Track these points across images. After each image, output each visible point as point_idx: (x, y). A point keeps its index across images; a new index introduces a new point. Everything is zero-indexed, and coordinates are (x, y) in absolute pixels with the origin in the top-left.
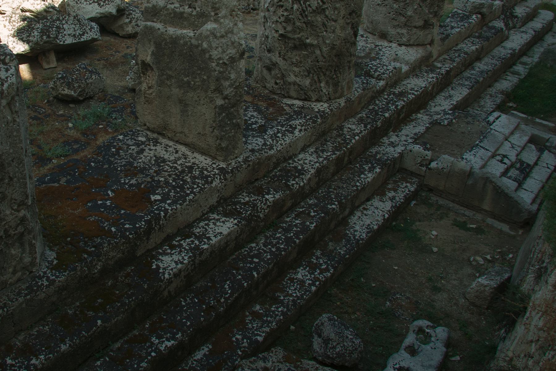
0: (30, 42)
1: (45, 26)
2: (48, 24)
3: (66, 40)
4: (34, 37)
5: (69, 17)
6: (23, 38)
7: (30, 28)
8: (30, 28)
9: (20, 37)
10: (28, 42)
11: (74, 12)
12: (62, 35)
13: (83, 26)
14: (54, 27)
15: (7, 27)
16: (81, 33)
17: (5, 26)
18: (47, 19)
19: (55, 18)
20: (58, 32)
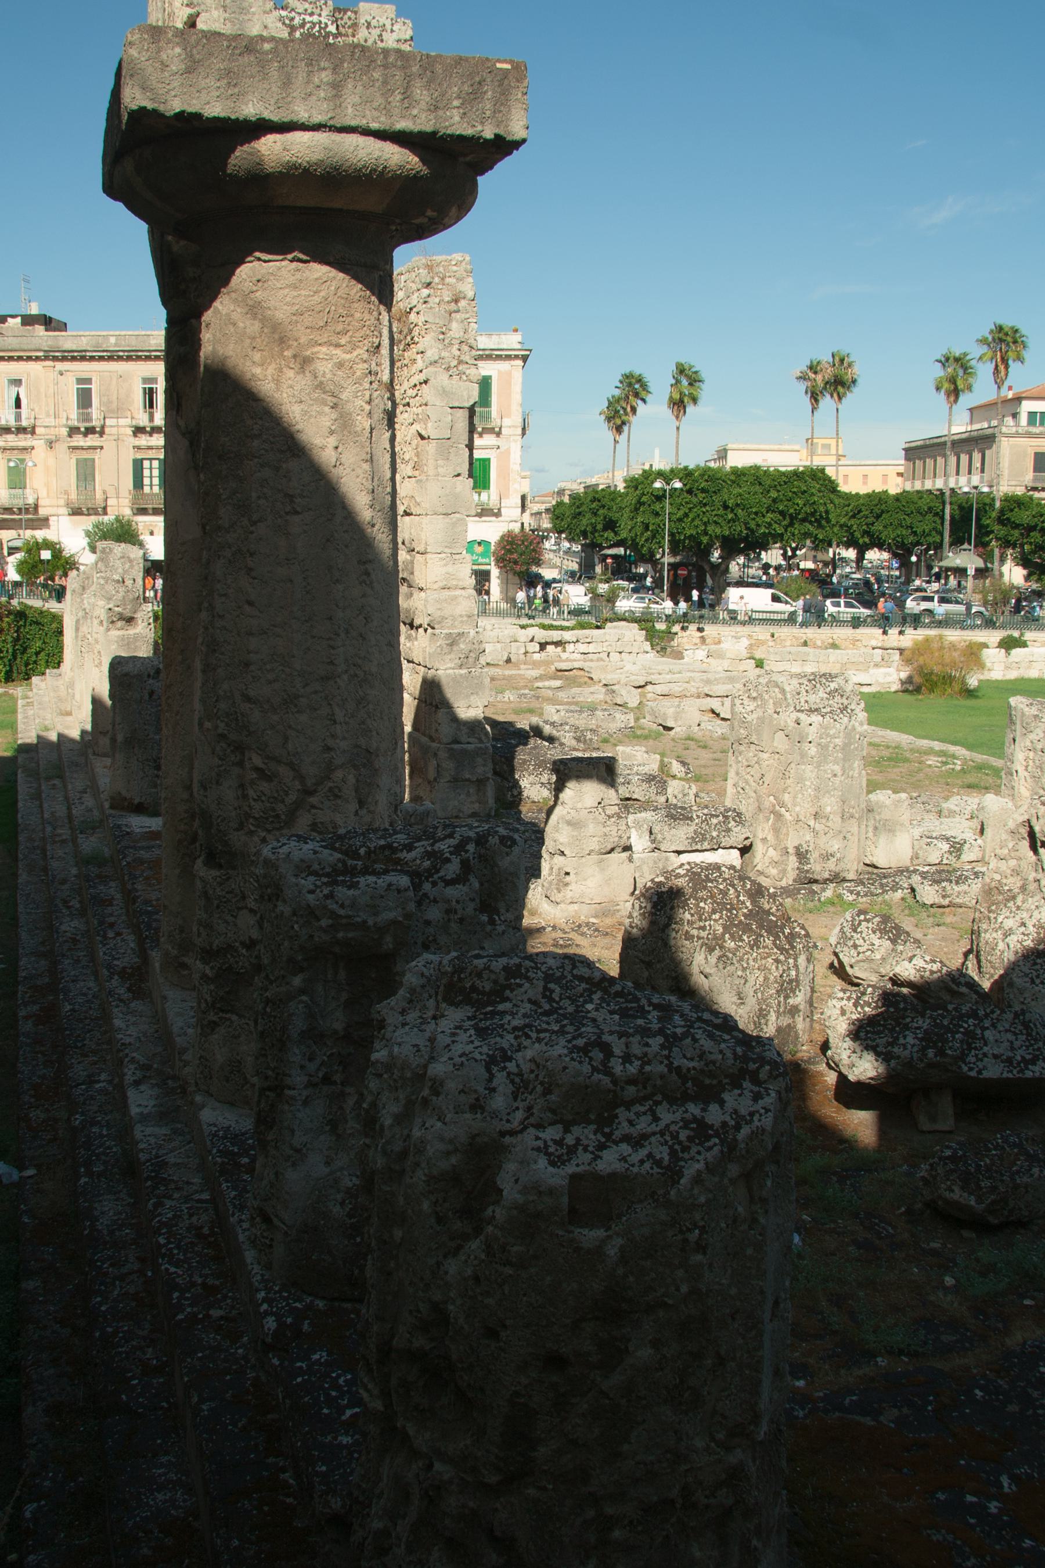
0: (892, 1058)
1: (936, 1025)
2: (946, 1023)
3: (985, 1068)
4: (905, 1048)
5: (1003, 1011)
6: (877, 1046)
7: (898, 1024)
8: (898, 1024)
9: (870, 1042)
10: (883, 1055)
11: (1023, 1003)
12: (976, 1056)
13: (1036, 1040)
14: (958, 1032)
15: (848, 1015)
16: (1028, 1057)
17: (843, 1012)
18: (945, 1009)
19: (964, 1009)
20: (969, 1045)
